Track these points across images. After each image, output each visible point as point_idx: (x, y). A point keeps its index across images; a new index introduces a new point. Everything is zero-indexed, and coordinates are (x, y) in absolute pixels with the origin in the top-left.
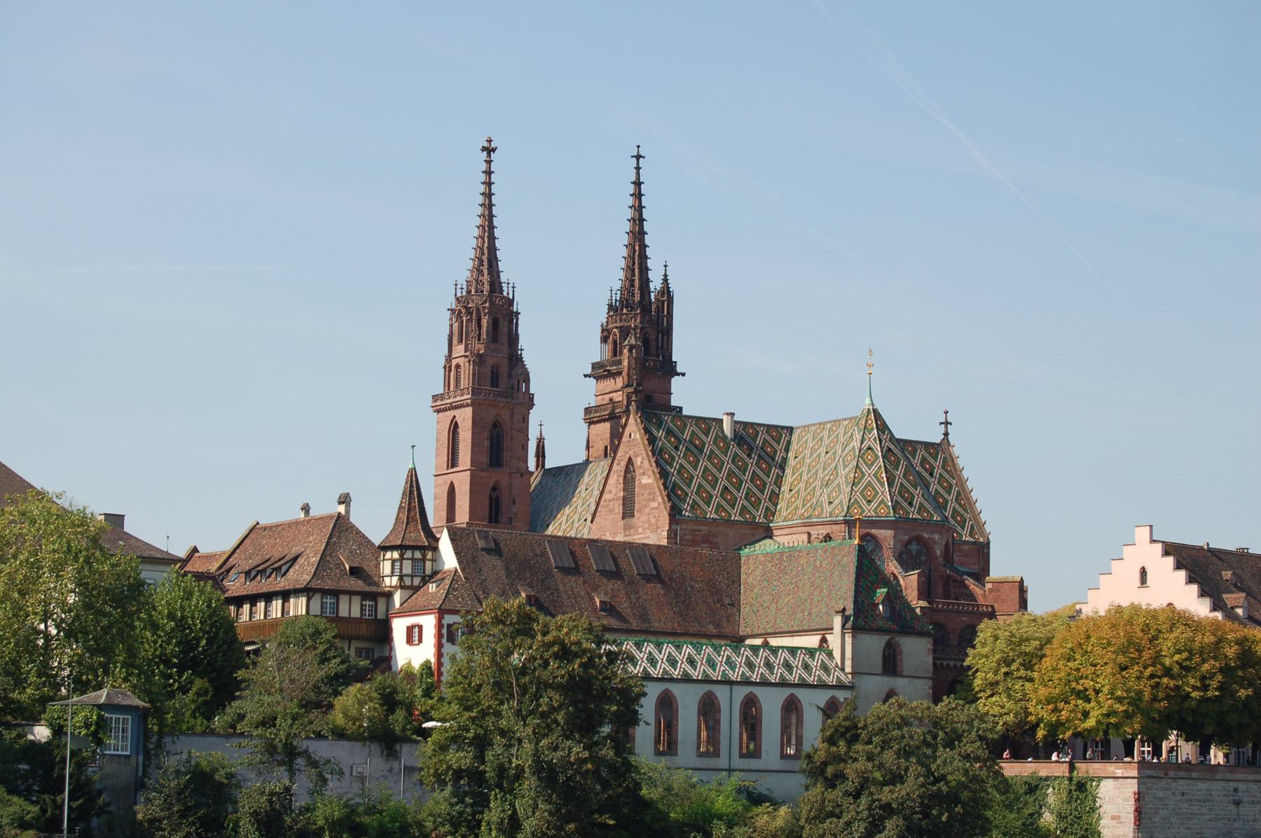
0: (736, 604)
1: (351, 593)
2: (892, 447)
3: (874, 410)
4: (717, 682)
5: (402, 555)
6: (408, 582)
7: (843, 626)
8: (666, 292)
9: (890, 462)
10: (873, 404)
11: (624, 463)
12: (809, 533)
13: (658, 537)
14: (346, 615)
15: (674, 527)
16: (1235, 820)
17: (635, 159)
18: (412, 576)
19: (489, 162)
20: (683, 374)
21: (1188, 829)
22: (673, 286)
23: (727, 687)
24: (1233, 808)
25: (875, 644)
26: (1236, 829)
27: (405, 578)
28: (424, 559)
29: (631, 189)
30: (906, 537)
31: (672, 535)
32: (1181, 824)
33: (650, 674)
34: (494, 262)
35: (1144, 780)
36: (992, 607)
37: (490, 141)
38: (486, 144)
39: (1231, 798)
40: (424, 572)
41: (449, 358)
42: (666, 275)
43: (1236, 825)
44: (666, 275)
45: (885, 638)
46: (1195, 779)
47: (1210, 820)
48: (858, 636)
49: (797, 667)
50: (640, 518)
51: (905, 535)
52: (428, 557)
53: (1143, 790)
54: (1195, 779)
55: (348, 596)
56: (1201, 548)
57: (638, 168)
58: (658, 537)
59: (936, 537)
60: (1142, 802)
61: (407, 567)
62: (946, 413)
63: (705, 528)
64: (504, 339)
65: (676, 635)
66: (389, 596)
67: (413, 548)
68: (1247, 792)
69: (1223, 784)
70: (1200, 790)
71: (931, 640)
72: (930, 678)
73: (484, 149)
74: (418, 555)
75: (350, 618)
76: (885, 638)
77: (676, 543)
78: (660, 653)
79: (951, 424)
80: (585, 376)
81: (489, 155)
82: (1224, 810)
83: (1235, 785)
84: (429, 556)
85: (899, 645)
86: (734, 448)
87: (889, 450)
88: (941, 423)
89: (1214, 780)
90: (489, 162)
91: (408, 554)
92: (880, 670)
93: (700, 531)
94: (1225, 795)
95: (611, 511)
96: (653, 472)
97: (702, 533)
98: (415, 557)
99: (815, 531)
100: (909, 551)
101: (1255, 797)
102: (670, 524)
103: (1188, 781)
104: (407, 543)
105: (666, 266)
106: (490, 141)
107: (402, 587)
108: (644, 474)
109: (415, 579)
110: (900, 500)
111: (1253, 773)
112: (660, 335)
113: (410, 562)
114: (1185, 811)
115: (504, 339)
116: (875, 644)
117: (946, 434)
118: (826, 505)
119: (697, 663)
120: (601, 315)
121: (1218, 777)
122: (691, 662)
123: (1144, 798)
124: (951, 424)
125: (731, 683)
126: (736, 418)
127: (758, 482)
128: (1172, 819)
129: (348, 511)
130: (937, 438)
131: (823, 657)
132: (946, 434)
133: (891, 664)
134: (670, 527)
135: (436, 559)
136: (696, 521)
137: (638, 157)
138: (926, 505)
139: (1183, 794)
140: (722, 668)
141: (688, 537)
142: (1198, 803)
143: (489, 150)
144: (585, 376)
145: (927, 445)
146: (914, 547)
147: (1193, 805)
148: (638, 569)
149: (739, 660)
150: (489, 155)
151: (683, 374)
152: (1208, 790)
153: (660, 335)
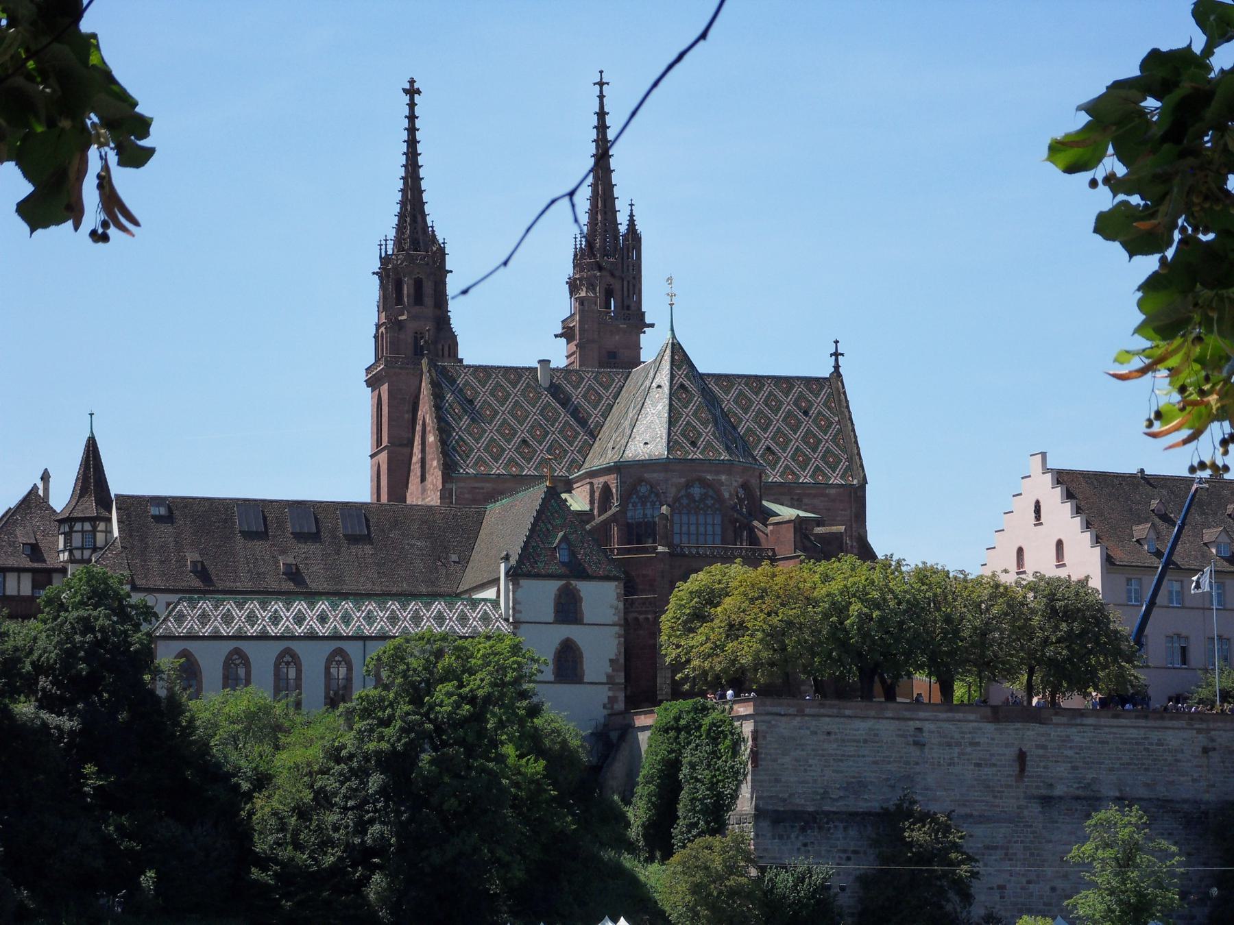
0: (464, 561)
1: (19, 570)
2: (687, 383)
3: (673, 344)
4: (348, 638)
5: (71, 528)
6: (77, 554)
7: (507, 574)
8: (634, 236)
9: (679, 400)
10: (674, 337)
11: (421, 422)
12: (591, 484)
13: (433, 499)
14: (15, 593)
15: (448, 486)
16: (917, 764)
17: (598, 87)
18: (82, 548)
19: (412, 105)
20: (652, 326)
21: (837, 772)
22: (640, 227)
23: (360, 643)
24: (915, 752)
25: (544, 593)
26: (919, 773)
27: (75, 552)
28: (94, 531)
29: (594, 121)
30: (683, 480)
31: (446, 495)
32: (825, 766)
33: (268, 632)
34: (419, 218)
35: (763, 718)
36: (773, 550)
37: (412, 82)
38: (407, 86)
39: (911, 739)
40: (95, 545)
41: (378, 326)
42: (631, 216)
43: (918, 769)
44: (631, 216)
45: (553, 586)
46: (850, 717)
47: (876, 763)
48: (523, 582)
49: (451, 619)
50: (429, 478)
51: (680, 478)
52: (99, 529)
53: (763, 727)
54: (850, 717)
55: (16, 574)
56: (1132, 476)
57: (601, 97)
58: (433, 499)
59: (723, 478)
60: (760, 741)
61: (77, 540)
62: (836, 342)
63: (488, 485)
64: (429, 301)
65: (382, 597)
66: (63, 571)
67: (83, 520)
68: (939, 733)
69: (897, 722)
70: (858, 730)
71: (622, 585)
72: (620, 625)
73: (405, 91)
74: (87, 526)
75: (19, 596)
76: (553, 586)
77: (452, 503)
78: (288, 611)
79: (842, 354)
80: (556, 336)
81: (412, 99)
82: (899, 752)
83: (918, 724)
84: (101, 526)
85: (578, 591)
86: (546, 398)
87: (682, 386)
88: (831, 355)
89: (882, 718)
90: (412, 105)
91: (78, 527)
92: (551, 619)
93: (483, 489)
94: (902, 736)
95: (416, 473)
96: (434, 428)
97: (485, 491)
98: (85, 529)
99: (595, 481)
100: (690, 496)
101: (952, 738)
102: (443, 483)
103: (837, 720)
104: (75, 515)
105: (631, 205)
106: (412, 82)
107: (72, 560)
108: (430, 432)
109: (85, 552)
110: (682, 440)
111: (946, 712)
112: (625, 283)
113: (80, 534)
114: (831, 752)
115: (429, 301)
116: (544, 593)
117: (837, 367)
118: (609, 452)
119: (329, 619)
120: (568, 270)
121: (891, 715)
122: (323, 619)
123: (765, 737)
124: (842, 354)
125: (364, 638)
126: (552, 365)
127: (569, 433)
128: (811, 762)
129: (46, 489)
130: (825, 371)
131: (488, 608)
132: (837, 367)
133: (568, 610)
134: (443, 486)
135: (109, 531)
136: (477, 477)
137: (601, 84)
138: (716, 444)
139: (829, 733)
140: (358, 623)
141: (467, 496)
142: (855, 744)
143: (412, 92)
144: (556, 336)
145: (808, 381)
146: (697, 491)
147: (846, 746)
148: (345, 528)
149: (382, 615)
150: (412, 99)
151: (652, 326)
152: (870, 729)
153: (625, 283)
